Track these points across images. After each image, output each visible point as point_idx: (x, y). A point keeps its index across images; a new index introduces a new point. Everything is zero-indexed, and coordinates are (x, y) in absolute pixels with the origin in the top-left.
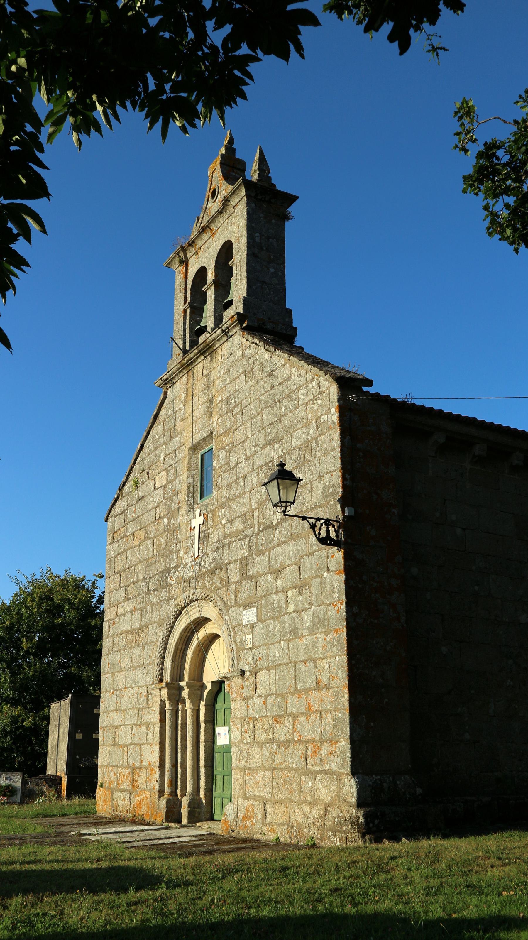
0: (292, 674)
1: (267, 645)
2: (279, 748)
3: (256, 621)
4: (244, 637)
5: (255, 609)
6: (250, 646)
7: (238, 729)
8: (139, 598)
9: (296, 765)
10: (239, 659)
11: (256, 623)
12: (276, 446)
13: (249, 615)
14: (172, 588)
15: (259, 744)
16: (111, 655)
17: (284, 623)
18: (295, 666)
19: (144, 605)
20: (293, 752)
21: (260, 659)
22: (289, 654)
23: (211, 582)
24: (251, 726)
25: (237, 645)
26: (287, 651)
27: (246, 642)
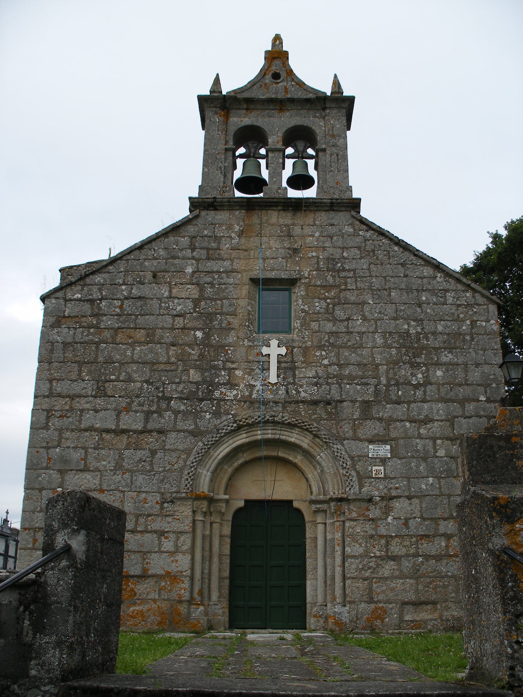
0: (445, 504)
1: (408, 479)
2: (427, 560)
3: (389, 456)
4: (370, 468)
5: (388, 447)
6: (382, 476)
7: (360, 544)
8: (137, 400)
9: (452, 573)
10: (361, 486)
11: (389, 458)
12: (413, 323)
13: (384, 450)
14: (226, 404)
15: (394, 558)
16: (57, 450)
17: (433, 463)
18: (449, 498)
19: (154, 408)
20: (447, 563)
21: (397, 488)
22: (440, 488)
23: (310, 412)
24: (383, 541)
25: (358, 473)
26: (438, 486)
27: (374, 473)
